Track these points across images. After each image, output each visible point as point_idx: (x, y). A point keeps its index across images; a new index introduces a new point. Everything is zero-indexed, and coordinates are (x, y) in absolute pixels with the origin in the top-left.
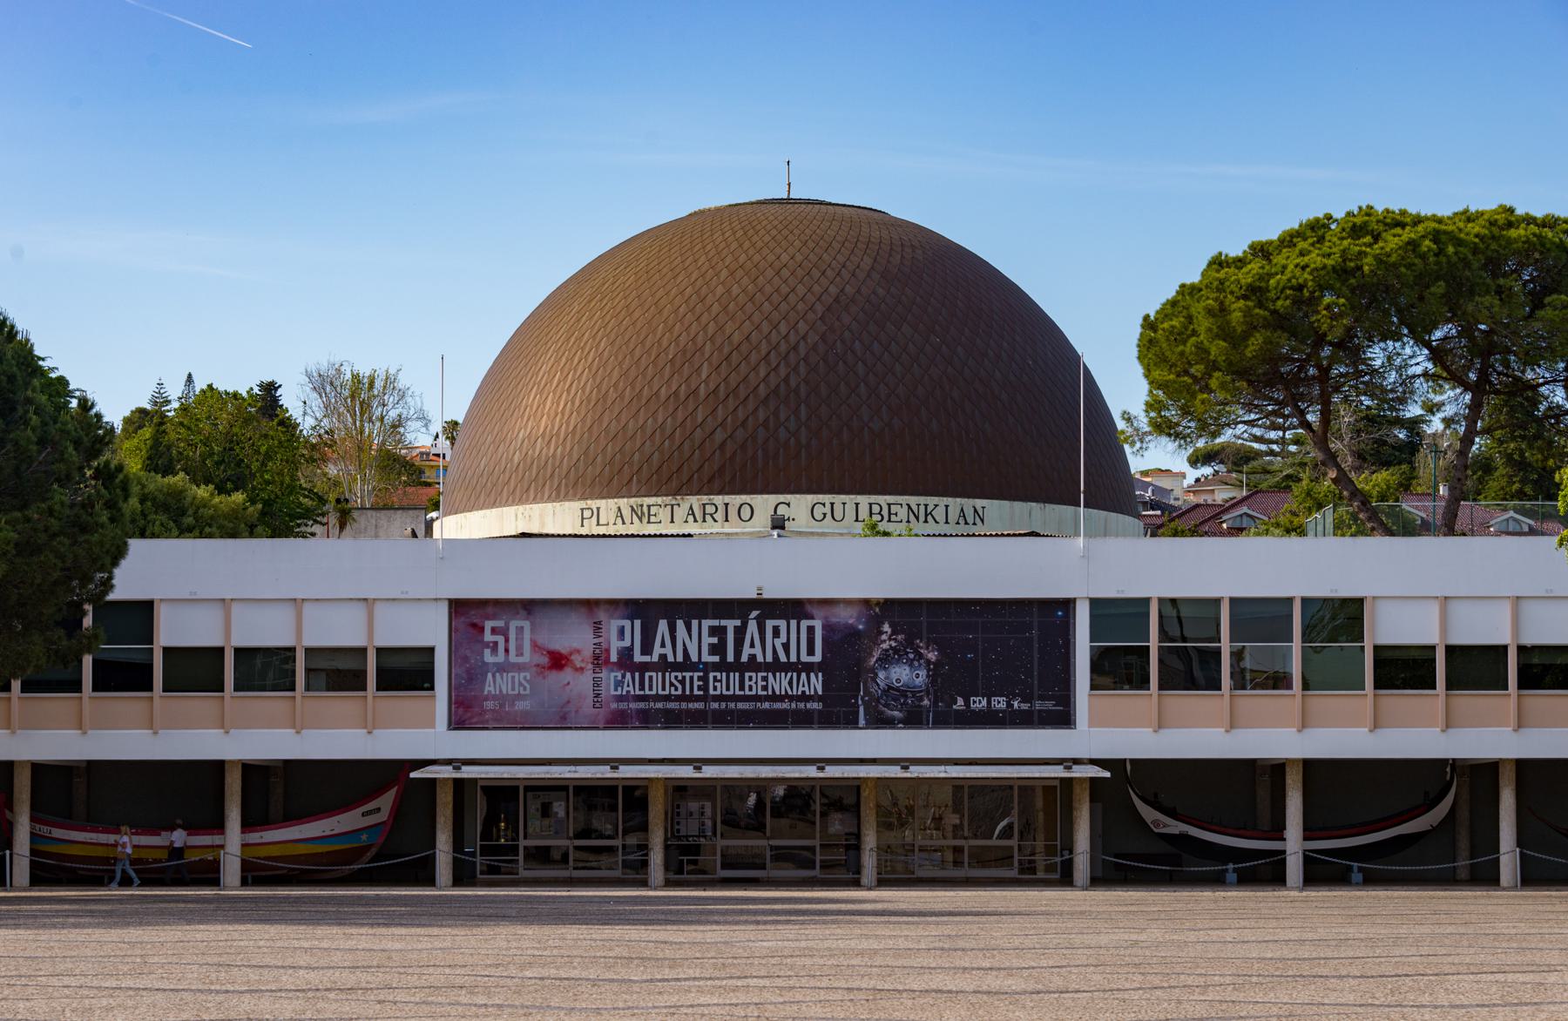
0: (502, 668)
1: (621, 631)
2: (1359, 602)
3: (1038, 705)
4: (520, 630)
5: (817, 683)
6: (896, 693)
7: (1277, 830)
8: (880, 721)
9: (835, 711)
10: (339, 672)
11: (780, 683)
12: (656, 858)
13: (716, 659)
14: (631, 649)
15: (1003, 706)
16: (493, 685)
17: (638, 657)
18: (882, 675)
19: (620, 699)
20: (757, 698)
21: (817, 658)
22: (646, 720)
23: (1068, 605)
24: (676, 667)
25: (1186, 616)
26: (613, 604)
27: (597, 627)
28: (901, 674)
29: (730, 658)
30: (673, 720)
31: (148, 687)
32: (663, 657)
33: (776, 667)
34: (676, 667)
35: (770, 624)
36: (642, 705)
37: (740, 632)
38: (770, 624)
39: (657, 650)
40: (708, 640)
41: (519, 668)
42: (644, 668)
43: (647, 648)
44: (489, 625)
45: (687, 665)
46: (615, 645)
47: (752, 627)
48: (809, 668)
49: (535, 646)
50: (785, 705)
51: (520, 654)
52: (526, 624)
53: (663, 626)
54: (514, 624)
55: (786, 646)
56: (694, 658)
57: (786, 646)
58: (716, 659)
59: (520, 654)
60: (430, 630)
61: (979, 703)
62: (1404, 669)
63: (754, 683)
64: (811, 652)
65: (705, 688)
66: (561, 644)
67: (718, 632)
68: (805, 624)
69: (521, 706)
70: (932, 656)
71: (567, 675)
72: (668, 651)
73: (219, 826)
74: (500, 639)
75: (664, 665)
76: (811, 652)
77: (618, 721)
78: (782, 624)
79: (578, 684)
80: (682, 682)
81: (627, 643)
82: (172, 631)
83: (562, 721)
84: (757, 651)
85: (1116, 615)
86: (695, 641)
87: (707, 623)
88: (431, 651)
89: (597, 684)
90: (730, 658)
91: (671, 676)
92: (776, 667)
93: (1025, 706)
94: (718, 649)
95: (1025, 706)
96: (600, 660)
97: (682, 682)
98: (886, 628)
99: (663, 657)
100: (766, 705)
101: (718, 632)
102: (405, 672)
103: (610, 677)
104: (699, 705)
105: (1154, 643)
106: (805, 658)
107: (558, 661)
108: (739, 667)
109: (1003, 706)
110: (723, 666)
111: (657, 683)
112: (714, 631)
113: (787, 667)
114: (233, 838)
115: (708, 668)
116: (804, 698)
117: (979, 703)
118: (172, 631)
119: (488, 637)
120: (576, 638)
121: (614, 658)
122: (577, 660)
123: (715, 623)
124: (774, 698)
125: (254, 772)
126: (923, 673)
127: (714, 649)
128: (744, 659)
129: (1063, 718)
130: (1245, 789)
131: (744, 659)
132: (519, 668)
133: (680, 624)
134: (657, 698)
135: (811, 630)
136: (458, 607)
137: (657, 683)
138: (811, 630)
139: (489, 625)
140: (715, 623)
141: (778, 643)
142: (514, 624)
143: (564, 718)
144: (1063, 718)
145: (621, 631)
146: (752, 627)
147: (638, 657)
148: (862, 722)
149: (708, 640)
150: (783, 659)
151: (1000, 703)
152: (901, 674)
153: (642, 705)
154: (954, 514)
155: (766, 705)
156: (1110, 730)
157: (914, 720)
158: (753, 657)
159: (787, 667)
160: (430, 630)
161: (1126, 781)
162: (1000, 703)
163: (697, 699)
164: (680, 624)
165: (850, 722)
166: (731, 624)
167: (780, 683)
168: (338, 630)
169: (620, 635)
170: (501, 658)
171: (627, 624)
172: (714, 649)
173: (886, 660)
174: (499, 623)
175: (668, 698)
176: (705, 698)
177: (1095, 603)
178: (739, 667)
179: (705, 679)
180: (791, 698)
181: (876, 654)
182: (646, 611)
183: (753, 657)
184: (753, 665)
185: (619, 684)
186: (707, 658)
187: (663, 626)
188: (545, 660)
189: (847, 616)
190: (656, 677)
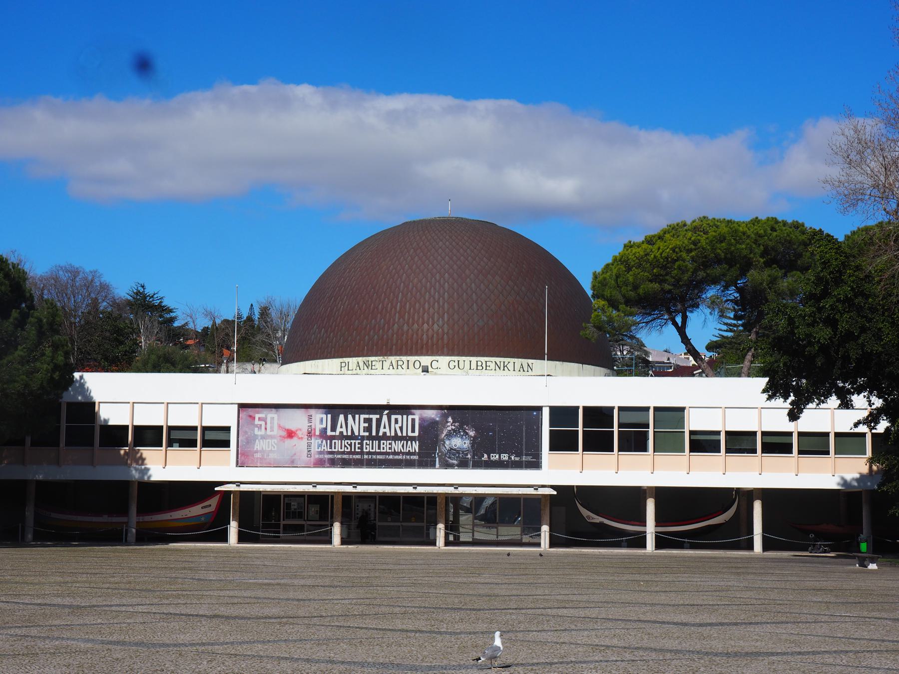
1: (322, 420)
2: (682, 410)
3: (524, 458)
5: (416, 446)
6: (453, 452)
8: (446, 465)
9: (425, 460)
13: (367, 434)
14: (326, 429)
16: (259, 445)
17: (329, 433)
18: (447, 442)
19: (320, 453)
21: (416, 434)
22: (333, 463)
23: (539, 409)
25: (598, 416)
27: (310, 418)
28: (458, 442)
29: (374, 434)
30: (346, 464)
31: (92, 445)
32: (341, 433)
33: (396, 438)
35: (393, 417)
36: (331, 456)
37: (379, 421)
38: (393, 417)
39: (339, 430)
40: (363, 425)
41: (272, 437)
42: (332, 438)
43: (334, 429)
45: (353, 437)
46: (318, 427)
48: (412, 439)
49: (279, 426)
50: (400, 457)
51: (272, 430)
52: (275, 416)
53: (342, 417)
55: (401, 428)
57: (401, 428)
58: (367, 434)
59: (272, 430)
61: (495, 457)
62: (704, 443)
63: (385, 446)
64: (413, 431)
65: (361, 448)
66: (293, 427)
67: (368, 421)
68: (410, 417)
69: (272, 456)
70: (472, 433)
71: (295, 441)
72: (344, 430)
73: (125, 512)
74: (263, 423)
75: (342, 437)
76: (413, 431)
77: (320, 464)
78: (399, 417)
79: (300, 445)
80: (351, 445)
81: (324, 426)
83: (292, 464)
84: (387, 430)
85: (563, 415)
86: (356, 424)
87: (363, 416)
89: (309, 445)
90: (374, 434)
91: (345, 442)
92: (396, 438)
93: (517, 459)
94: (368, 429)
95: (517, 459)
96: (310, 434)
97: (351, 445)
98: (450, 419)
99: (341, 433)
100: (391, 457)
101: (368, 421)
102: (215, 438)
103: (315, 442)
104: (358, 457)
105: (580, 429)
106: (410, 434)
107: (291, 434)
108: (378, 438)
110: (370, 438)
111: (338, 446)
112: (366, 420)
113: (402, 438)
114: (133, 517)
115: (363, 438)
116: (409, 453)
117: (495, 457)
119: (257, 422)
120: (298, 421)
121: (318, 433)
122: (299, 434)
123: (367, 416)
124: (395, 453)
126: (468, 442)
127: (366, 429)
128: (381, 434)
129: (536, 465)
130: (628, 501)
131: (381, 434)
132: (272, 437)
133: (350, 417)
134: (338, 453)
135: (413, 420)
136: (242, 406)
137: (338, 446)
138: (413, 420)
139: (257, 416)
140: (367, 416)
141: (397, 426)
143: (293, 462)
144: (536, 465)
145: (322, 420)
147: (329, 433)
148: (437, 465)
149: (363, 425)
150: (399, 434)
151: (505, 457)
152: (458, 442)
153: (331, 456)
155: (391, 457)
157: (463, 464)
158: (385, 433)
159: (402, 438)
160: (227, 417)
161: (567, 496)
162: (505, 457)
163: (358, 453)
164: (350, 417)
165: (433, 465)
166: (374, 417)
167: (398, 446)
168: (183, 417)
169: (321, 420)
170: (262, 432)
171: (324, 416)
172: (366, 429)
173: (450, 435)
175: (343, 453)
176: (362, 453)
178: (378, 438)
179: (361, 444)
180: (403, 454)
181: (445, 432)
182: (333, 410)
183: (385, 433)
184: (385, 437)
185: (320, 446)
186: (362, 433)
187: (342, 417)
188: (284, 434)
189: (431, 414)
190: (338, 442)
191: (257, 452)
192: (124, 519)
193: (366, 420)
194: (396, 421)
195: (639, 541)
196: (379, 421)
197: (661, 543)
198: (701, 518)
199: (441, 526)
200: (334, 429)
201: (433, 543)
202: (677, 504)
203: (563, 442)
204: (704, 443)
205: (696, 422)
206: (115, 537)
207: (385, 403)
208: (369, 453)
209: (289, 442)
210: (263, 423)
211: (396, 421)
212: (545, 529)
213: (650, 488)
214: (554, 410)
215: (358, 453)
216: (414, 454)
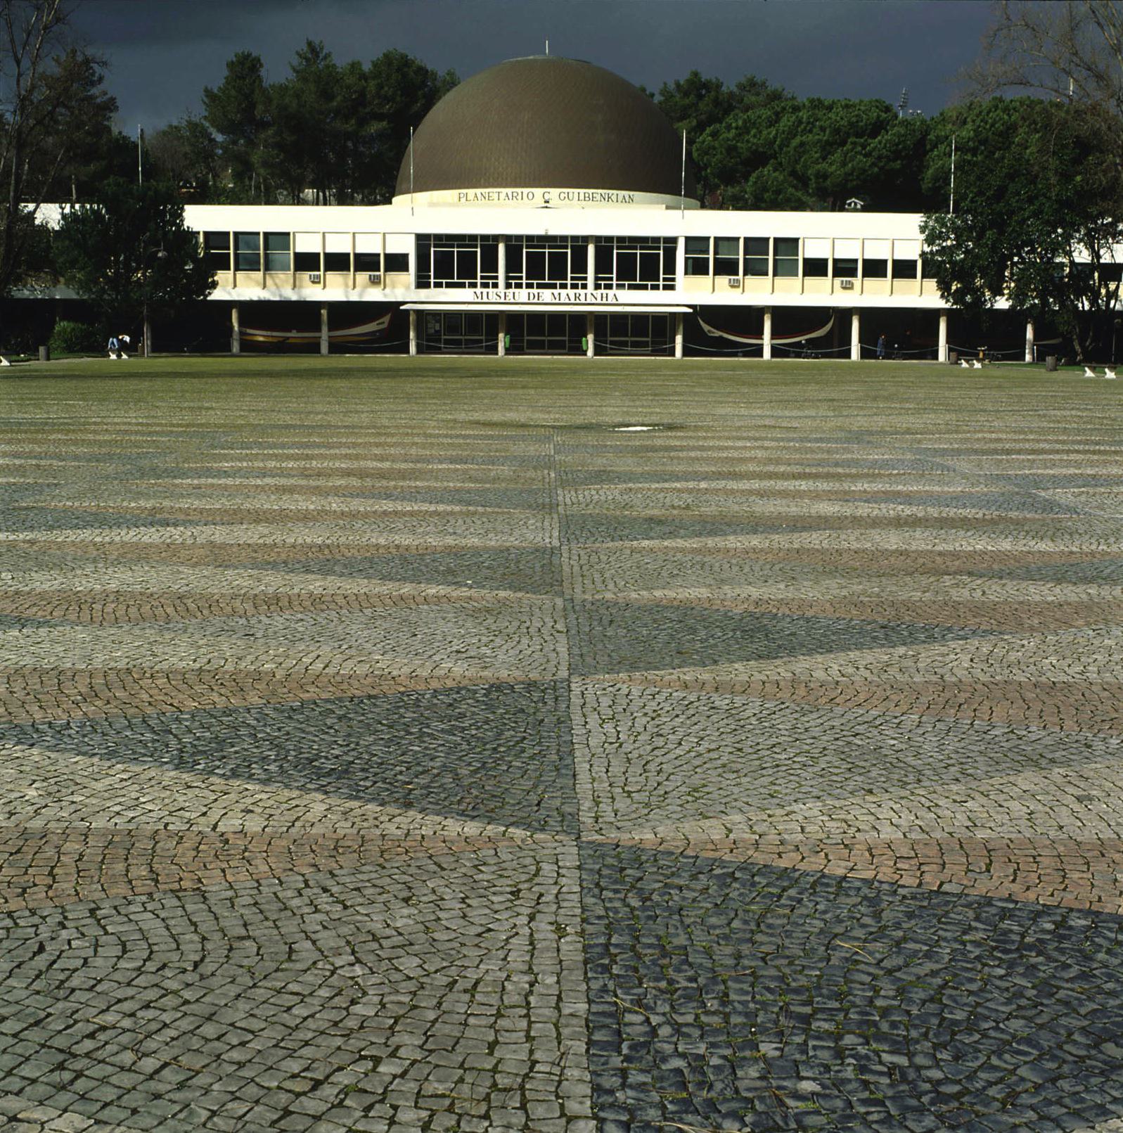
2: (797, 240)
7: (760, 334)
10: (366, 262)
60: (407, 247)
62: (815, 268)
73: (319, 330)
85: (696, 243)
88: (406, 256)
102: (396, 263)
114: (325, 334)
125: (333, 306)
130: (747, 319)
154: (503, 196)
156: (692, 291)
177: (688, 239)
192: (317, 334)
195: (758, 351)
197: (776, 352)
198: (810, 332)
199: (590, 337)
201: (584, 353)
202: (790, 320)
203: (696, 267)
204: (815, 268)
205: (811, 250)
206: (312, 348)
207: (542, 233)
212: (679, 339)
213: (768, 307)
214: (688, 240)
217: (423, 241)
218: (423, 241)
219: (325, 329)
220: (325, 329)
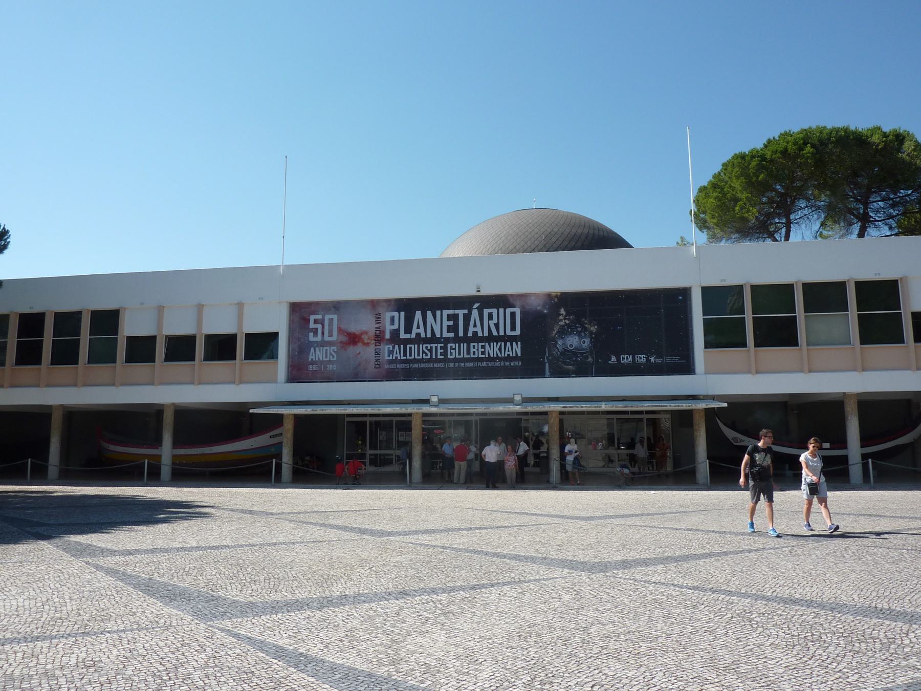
0: (323, 344)
1: (392, 319)
3: (669, 359)
4: (331, 320)
5: (517, 349)
9: (530, 367)
10: (221, 347)
11: (493, 350)
12: (417, 463)
13: (452, 335)
14: (398, 330)
15: (643, 360)
17: (403, 335)
18: (560, 342)
19: (391, 362)
20: (478, 360)
21: (518, 332)
23: (685, 293)
24: (426, 341)
25: (775, 296)
26: (388, 301)
27: (378, 318)
28: (573, 341)
29: (461, 334)
32: (418, 335)
33: (490, 339)
34: (426, 341)
35: (486, 312)
36: (405, 366)
37: (467, 318)
38: (486, 312)
39: (415, 331)
40: (446, 323)
41: (330, 344)
42: (406, 342)
43: (408, 330)
44: (312, 318)
45: (433, 339)
46: (388, 328)
47: (475, 313)
48: (512, 339)
49: (340, 330)
51: (331, 335)
53: (418, 315)
54: (327, 317)
55: (497, 326)
56: (438, 335)
57: (497, 326)
58: (452, 335)
59: (331, 335)
60: (276, 322)
61: (627, 359)
63: (476, 350)
64: (513, 328)
65: (445, 354)
66: (354, 328)
68: (509, 311)
70: (593, 329)
71: (359, 348)
72: (421, 331)
74: (319, 327)
75: (419, 340)
76: (513, 328)
77: (391, 376)
78: (494, 311)
79: (367, 353)
80: (430, 350)
81: (396, 327)
82: (133, 326)
83: (356, 377)
84: (478, 329)
86: (438, 324)
87: (445, 312)
88: (275, 335)
89: (377, 353)
90: (461, 334)
91: (423, 347)
92: (490, 339)
93: (659, 361)
94: (453, 329)
95: (659, 361)
97: (430, 350)
98: (562, 311)
99: (418, 335)
100: (485, 364)
101: (454, 318)
104: (442, 365)
106: (509, 333)
107: (354, 339)
108: (467, 340)
109: (643, 360)
110: (457, 340)
112: (450, 317)
113: (498, 339)
115: (447, 340)
116: (508, 358)
117: (627, 359)
118: (133, 326)
119: (312, 325)
121: (388, 336)
122: (365, 338)
123: (451, 312)
124: (490, 359)
126: (587, 340)
127: (449, 329)
128: (470, 334)
129: (687, 368)
131: (470, 334)
133: (429, 313)
134: (415, 361)
135: (513, 315)
136: (295, 308)
137: (416, 352)
138: (513, 315)
139: (312, 318)
140: (451, 312)
141: (492, 323)
142: (327, 317)
145: (392, 319)
146: (475, 313)
147: (403, 335)
148: (547, 373)
149: (446, 323)
150: (495, 333)
151: (642, 359)
152: (573, 341)
153: (405, 366)
155: (485, 364)
157: (582, 371)
158: (475, 333)
159: (498, 339)
160: (276, 322)
162: (642, 359)
163: (440, 361)
164: (429, 313)
165: (540, 374)
166: (461, 313)
167: (493, 350)
170: (319, 338)
171: (396, 314)
172: (449, 329)
173: (563, 332)
174: (319, 317)
175: (421, 361)
176: (446, 360)
178: (467, 340)
179: (444, 348)
180: (501, 359)
181: (556, 330)
183: (475, 333)
184: (476, 338)
185: (391, 352)
186: (445, 334)
187: (418, 315)
189: (536, 304)
190: (414, 347)
191: (313, 363)
193: (450, 317)
194: (490, 317)
196: (467, 318)
200: (408, 330)
203: (724, 335)
208: (455, 360)
209: (352, 350)
210: (319, 327)
211: (490, 317)
215: (440, 361)
216: (516, 358)
217: (301, 313)
218: (301, 313)
219: (167, 439)
220: (167, 439)
